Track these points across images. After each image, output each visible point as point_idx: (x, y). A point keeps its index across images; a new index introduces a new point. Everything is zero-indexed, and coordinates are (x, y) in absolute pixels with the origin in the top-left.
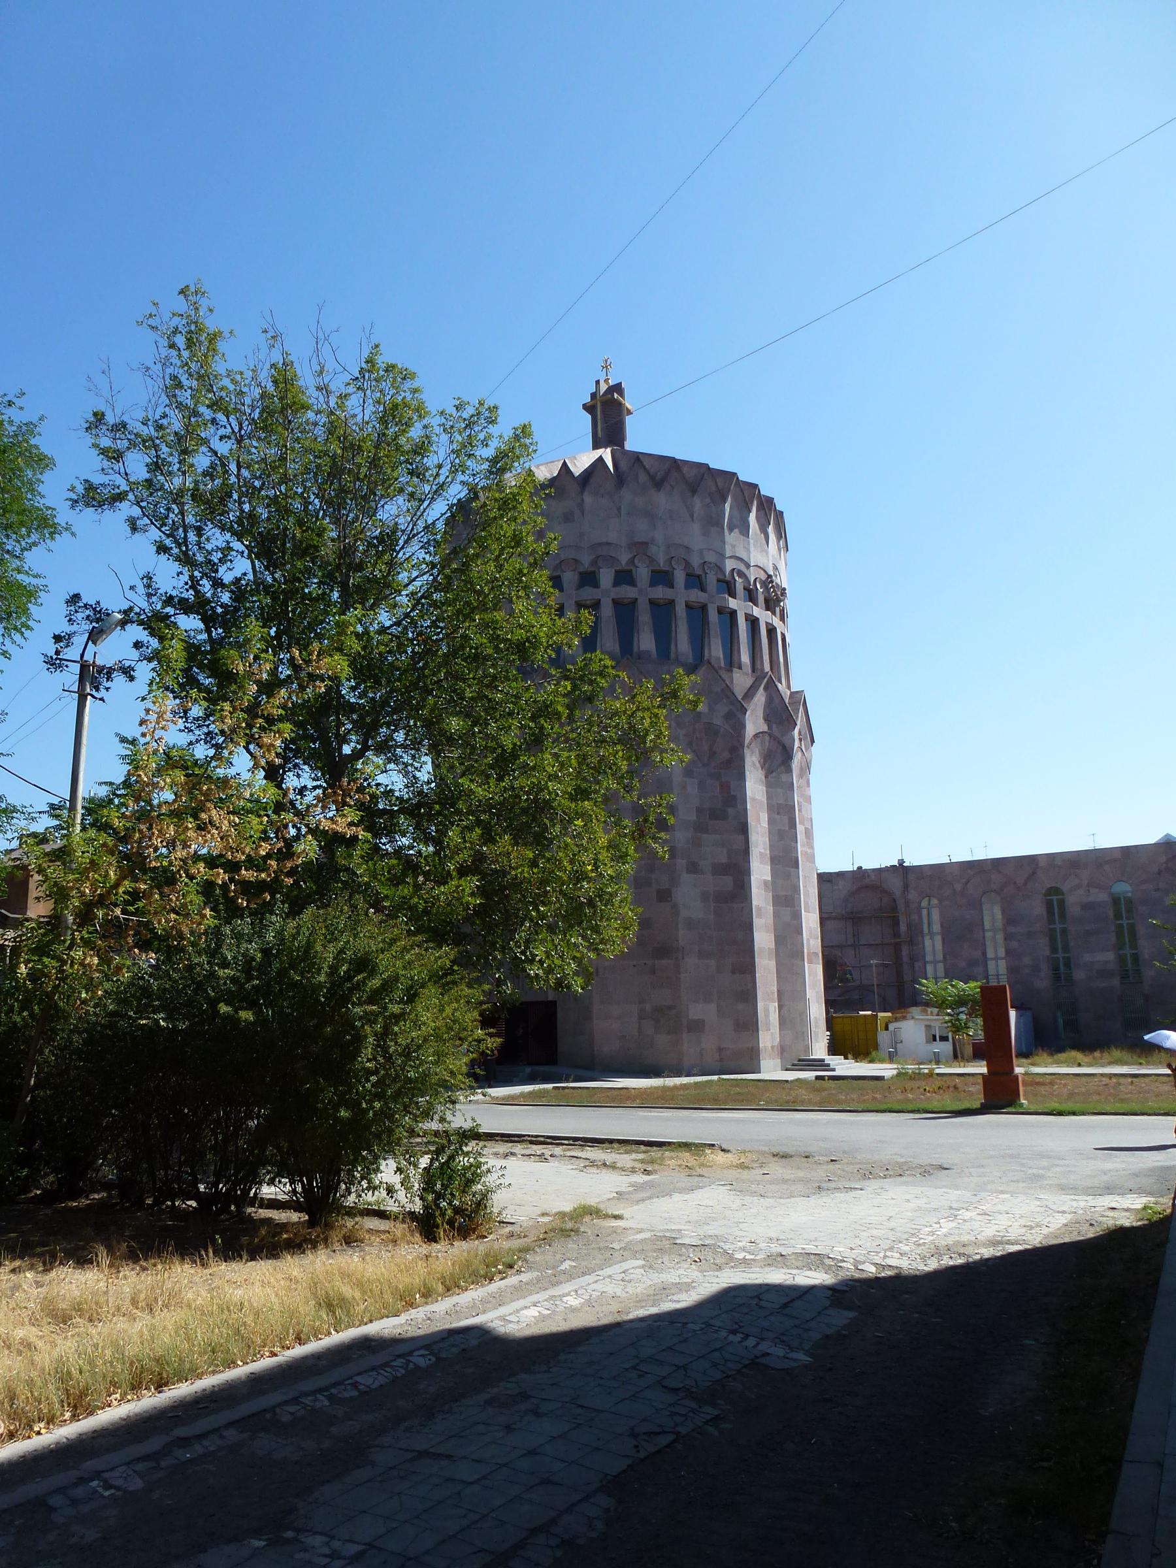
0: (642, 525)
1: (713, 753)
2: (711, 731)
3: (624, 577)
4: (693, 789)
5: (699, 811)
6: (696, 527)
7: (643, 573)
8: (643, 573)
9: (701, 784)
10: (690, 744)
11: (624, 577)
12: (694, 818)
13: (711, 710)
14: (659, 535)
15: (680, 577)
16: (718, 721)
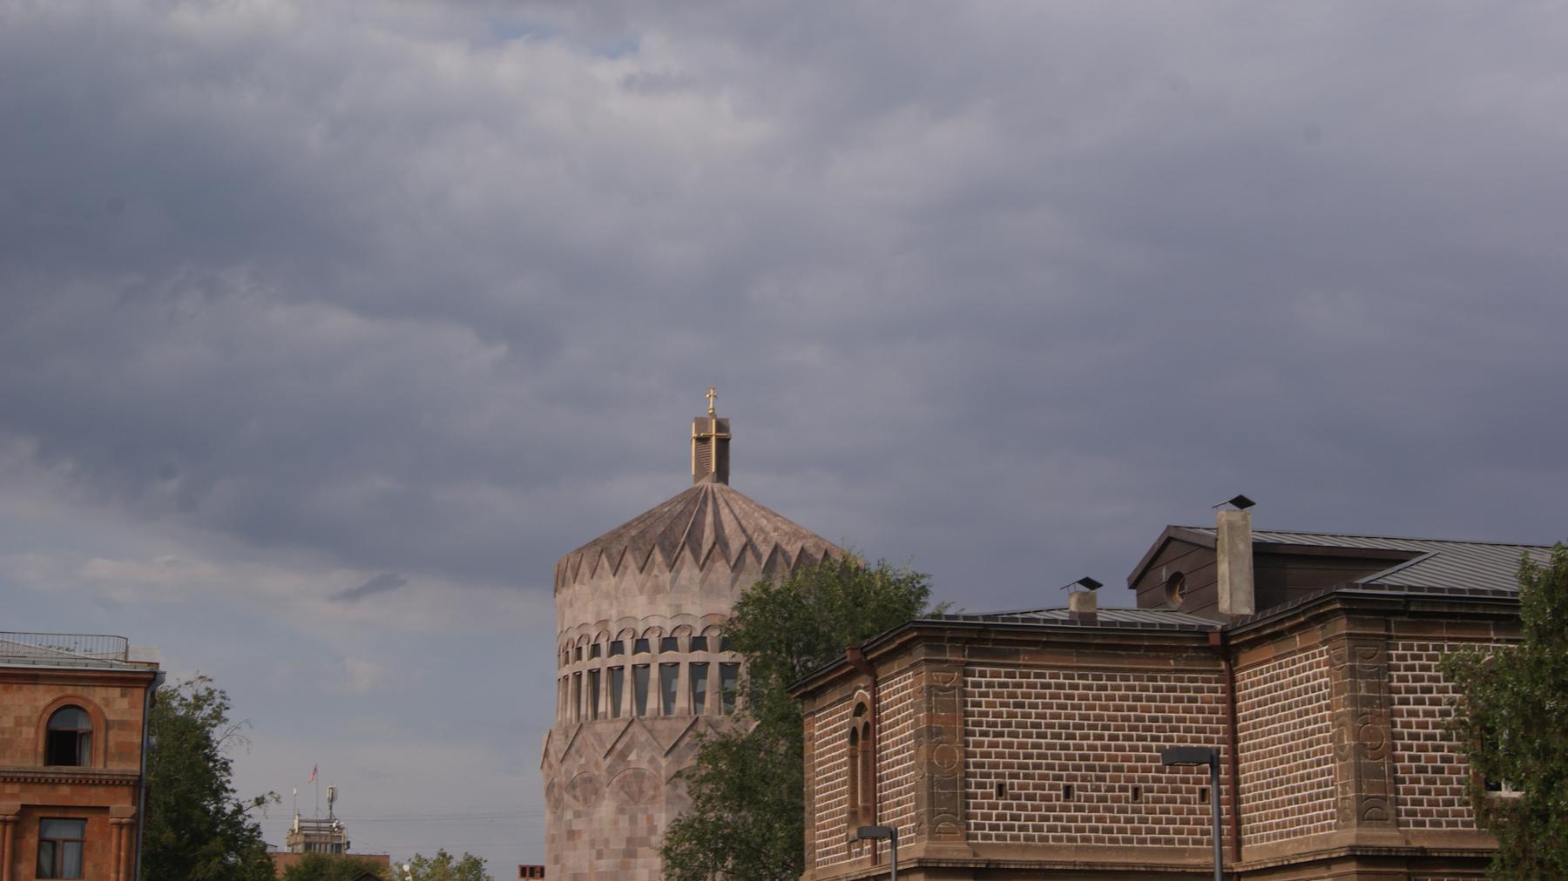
0: (605, 605)
1: (641, 792)
2: (639, 775)
3: (595, 651)
4: (624, 822)
5: (630, 841)
6: (642, 600)
7: (604, 647)
8: (604, 647)
9: (633, 820)
10: (622, 787)
11: (595, 651)
12: (624, 846)
13: (639, 757)
14: (614, 613)
15: (628, 645)
16: (644, 765)
